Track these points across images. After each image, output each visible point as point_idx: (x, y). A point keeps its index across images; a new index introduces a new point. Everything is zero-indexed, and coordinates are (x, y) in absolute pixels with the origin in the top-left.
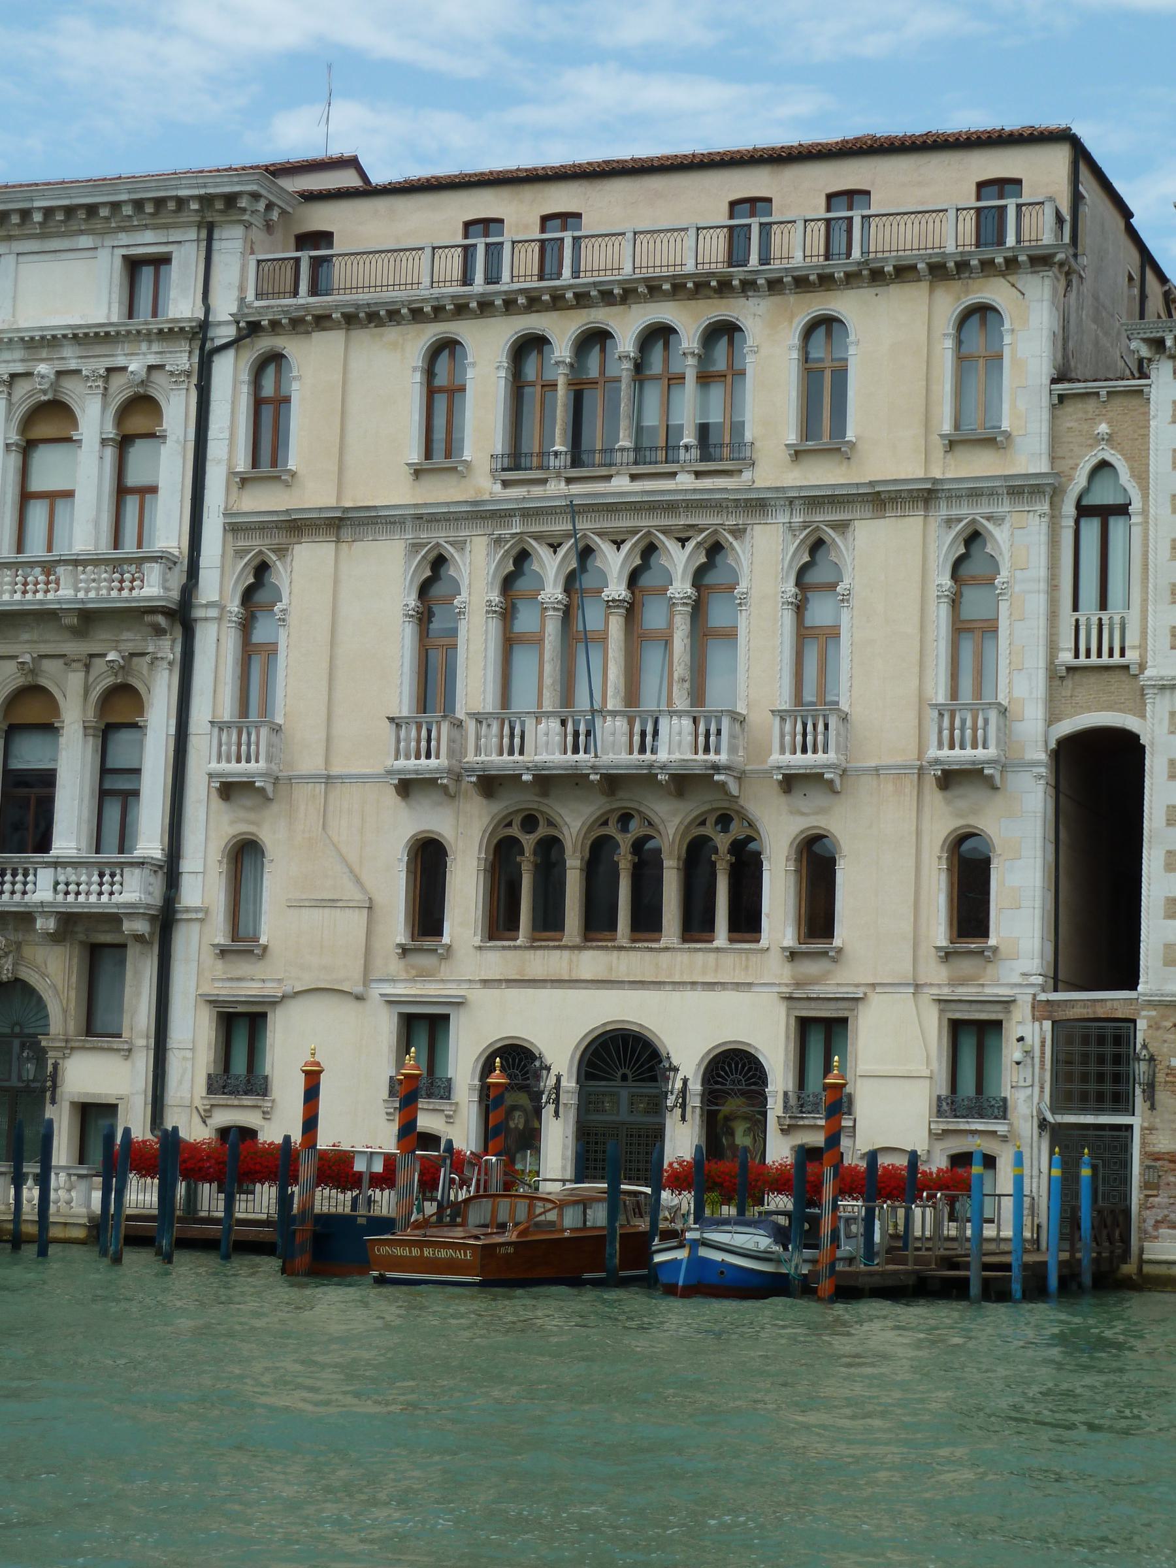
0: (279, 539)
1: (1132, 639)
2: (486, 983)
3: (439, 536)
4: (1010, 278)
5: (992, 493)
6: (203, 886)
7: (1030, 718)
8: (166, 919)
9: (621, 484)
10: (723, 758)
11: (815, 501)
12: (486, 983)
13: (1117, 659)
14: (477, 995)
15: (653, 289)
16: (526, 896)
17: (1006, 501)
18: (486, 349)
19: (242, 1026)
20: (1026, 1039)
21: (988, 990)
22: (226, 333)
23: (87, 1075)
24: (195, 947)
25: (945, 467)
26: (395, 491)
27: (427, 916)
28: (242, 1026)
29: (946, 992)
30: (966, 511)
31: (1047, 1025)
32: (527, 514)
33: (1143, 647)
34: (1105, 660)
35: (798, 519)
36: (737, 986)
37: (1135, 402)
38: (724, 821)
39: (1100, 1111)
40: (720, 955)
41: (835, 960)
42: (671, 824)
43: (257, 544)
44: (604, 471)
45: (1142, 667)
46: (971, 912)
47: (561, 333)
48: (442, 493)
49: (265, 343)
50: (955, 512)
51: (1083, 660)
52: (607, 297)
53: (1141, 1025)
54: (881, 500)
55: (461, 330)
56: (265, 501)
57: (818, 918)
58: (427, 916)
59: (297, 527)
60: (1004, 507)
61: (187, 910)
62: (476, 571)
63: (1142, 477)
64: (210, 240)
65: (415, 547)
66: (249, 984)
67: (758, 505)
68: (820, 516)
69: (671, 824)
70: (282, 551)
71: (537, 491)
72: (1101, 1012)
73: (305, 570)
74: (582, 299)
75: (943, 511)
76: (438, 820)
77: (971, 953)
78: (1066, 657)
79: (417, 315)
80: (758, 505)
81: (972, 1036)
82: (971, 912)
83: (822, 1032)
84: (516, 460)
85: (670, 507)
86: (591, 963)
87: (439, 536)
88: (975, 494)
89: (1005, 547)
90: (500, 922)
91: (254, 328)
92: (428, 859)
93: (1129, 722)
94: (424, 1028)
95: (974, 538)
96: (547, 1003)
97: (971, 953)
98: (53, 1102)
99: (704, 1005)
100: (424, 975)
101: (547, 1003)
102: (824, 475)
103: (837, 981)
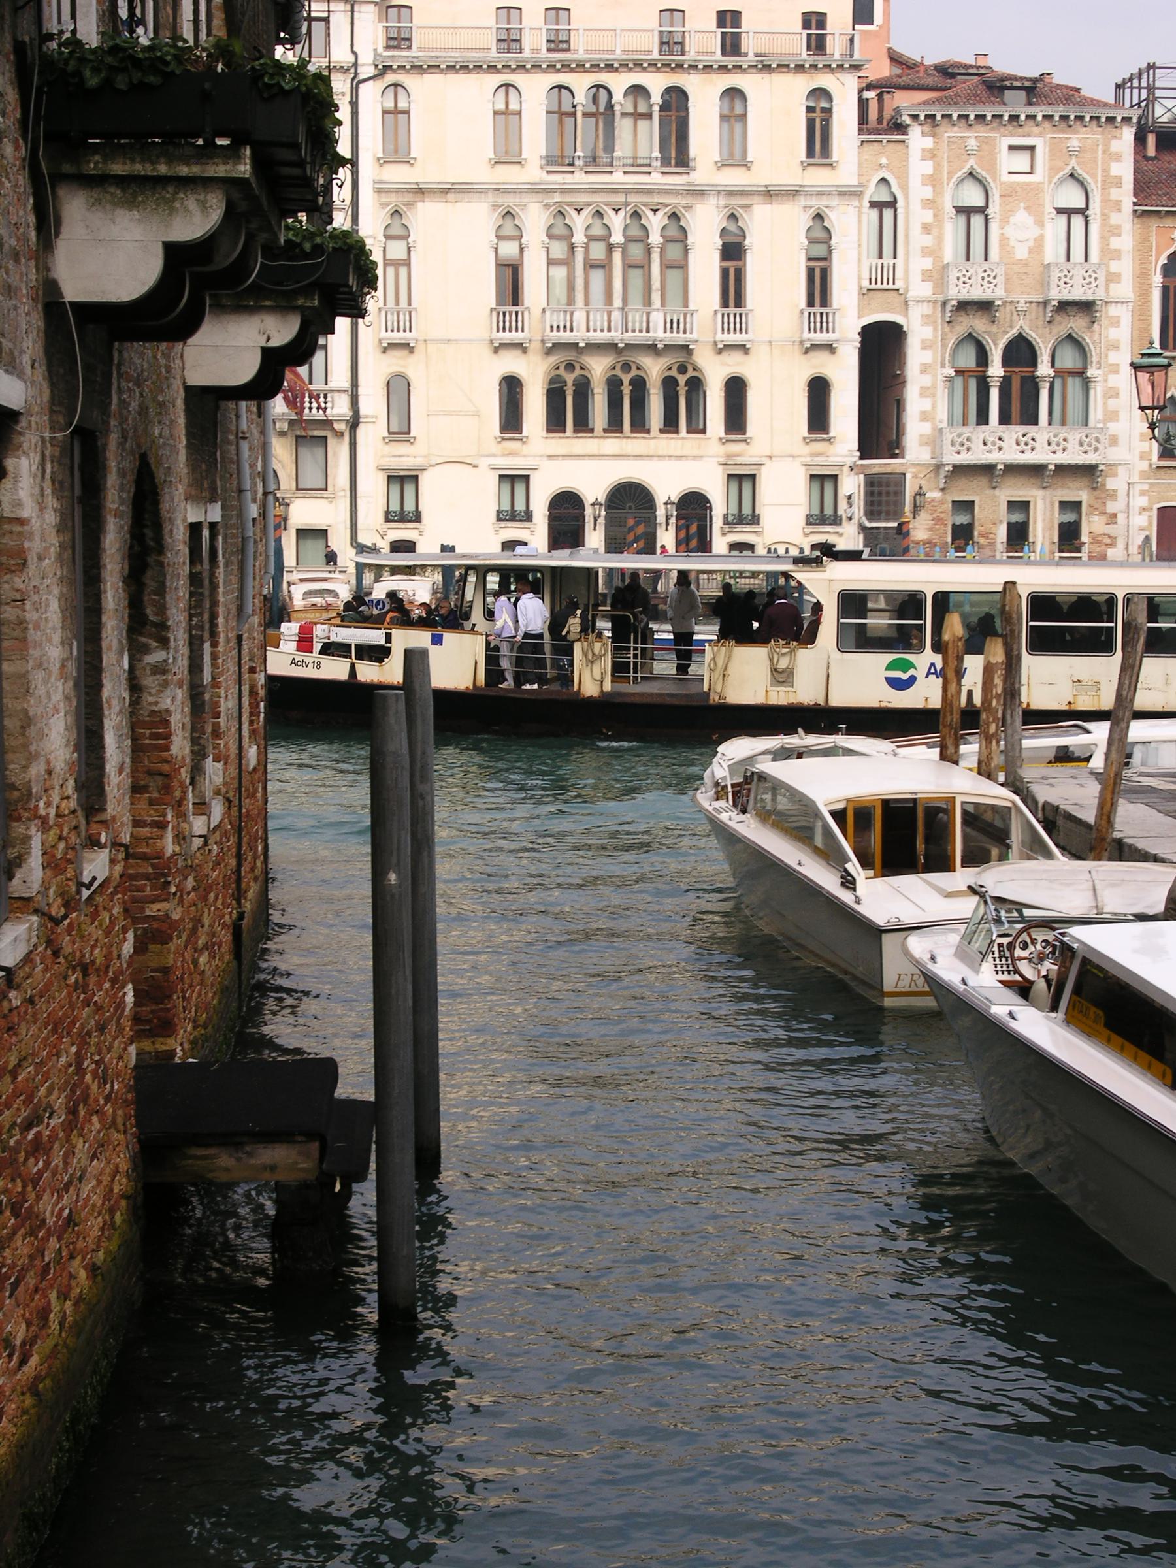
0: (408, 197)
1: (898, 274)
2: (550, 457)
3: (510, 201)
4: (838, 75)
5: (829, 194)
6: (373, 403)
7: (849, 318)
8: (354, 423)
9: (618, 178)
10: (694, 336)
11: (731, 193)
12: (550, 457)
13: (891, 286)
14: (546, 465)
15: (638, 65)
16: (567, 408)
17: (836, 198)
18: (535, 91)
19: (403, 480)
20: (851, 485)
21: (831, 459)
22: (366, 71)
23: (304, 512)
24: (371, 436)
25: (803, 178)
26: (482, 173)
27: (511, 420)
28: (403, 480)
29: (808, 460)
30: (816, 203)
31: (862, 477)
32: (563, 191)
33: (906, 279)
34: (885, 286)
35: (722, 202)
36: (695, 457)
37: (899, 147)
38: (682, 369)
39: (879, 520)
40: (683, 441)
41: (748, 444)
42: (654, 369)
43: (394, 200)
44: (609, 169)
45: (907, 290)
46: (818, 419)
47: (581, 84)
48: (509, 175)
49: (390, 78)
50: (809, 203)
51: (873, 286)
52: (610, 67)
53: (908, 476)
54: (769, 194)
55: (517, 79)
56: (398, 175)
57: (736, 419)
58: (511, 420)
59: (420, 191)
60: (835, 201)
61: (367, 417)
62: (535, 220)
63: (905, 188)
64: (353, 11)
65: (495, 207)
66: (404, 457)
67: (701, 193)
68: (737, 201)
69: (654, 369)
70: (410, 205)
71: (569, 176)
72: (888, 470)
73: (425, 217)
74: (595, 67)
75: (802, 201)
76: (512, 364)
77: (824, 440)
78: (865, 283)
79: (492, 69)
80: (701, 193)
81: (823, 481)
82: (818, 419)
83: (743, 481)
84: (559, 160)
85: (649, 192)
86: (612, 444)
87: (510, 201)
88: (820, 194)
89: (835, 223)
90: (555, 423)
91: (387, 69)
92: (512, 387)
93: (898, 319)
94: (515, 481)
95: (819, 217)
96: (590, 467)
97: (824, 440)
98: (285, 529)
99: (672, 467)
100: (511, 454)
101: (590, 467)
102: (734, 178)
103: (746, 454)
